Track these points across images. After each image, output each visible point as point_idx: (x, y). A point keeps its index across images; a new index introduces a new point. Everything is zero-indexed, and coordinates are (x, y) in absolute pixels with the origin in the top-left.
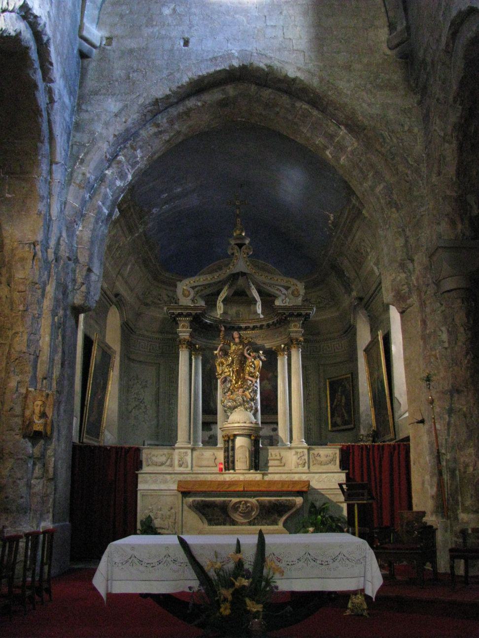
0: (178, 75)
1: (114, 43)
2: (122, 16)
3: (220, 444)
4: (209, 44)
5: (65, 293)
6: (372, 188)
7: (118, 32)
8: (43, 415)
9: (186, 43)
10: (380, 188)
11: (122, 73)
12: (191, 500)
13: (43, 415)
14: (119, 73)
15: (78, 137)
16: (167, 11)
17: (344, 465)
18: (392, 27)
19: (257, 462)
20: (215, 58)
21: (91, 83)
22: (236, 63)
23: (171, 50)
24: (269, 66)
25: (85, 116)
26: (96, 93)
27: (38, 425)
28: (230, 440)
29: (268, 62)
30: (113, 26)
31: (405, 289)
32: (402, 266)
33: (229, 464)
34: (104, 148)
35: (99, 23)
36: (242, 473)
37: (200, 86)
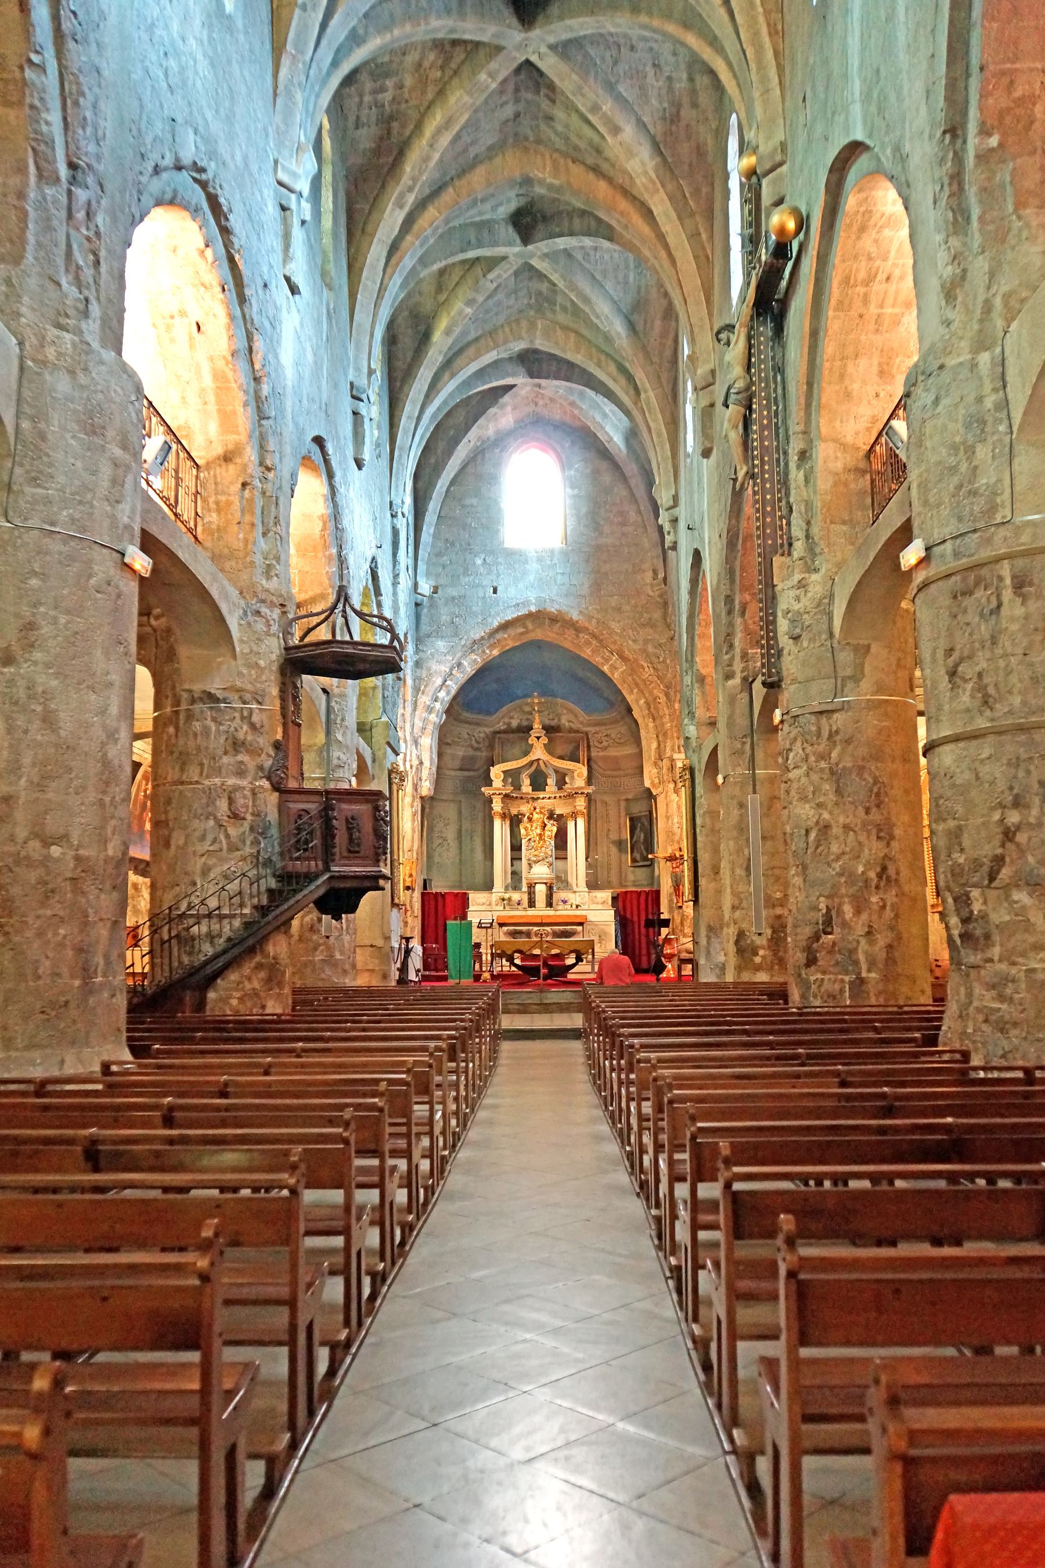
0: (490, 620)
1: (440, 591)
2: (444, 567)
3: (525, 889)
4: (512, 592)
5: (416, 790)
6: (637, 701)
7: (442, 581)
8: (411, 875)
9: (495, 591)
10: (642, 702)
11: (448, 619)
12: (505, 929)
13: (411, 875)
14: (445, 618)
16: (479, 561)
18: (655, 572)
20: (518, 605)
21: (425, 628)
22: (533, 609)
24: (559, 611)
25: (421, 654)
26: (429, 636)
28: (531, 887)
29: (557, 607)
30: (438, 575)
31: (656, 781)
32: (655, 764)
33: (532, 904)
34: (439, 681)
35: (428, 575)
36: (541, 910)
37: (505, 626)
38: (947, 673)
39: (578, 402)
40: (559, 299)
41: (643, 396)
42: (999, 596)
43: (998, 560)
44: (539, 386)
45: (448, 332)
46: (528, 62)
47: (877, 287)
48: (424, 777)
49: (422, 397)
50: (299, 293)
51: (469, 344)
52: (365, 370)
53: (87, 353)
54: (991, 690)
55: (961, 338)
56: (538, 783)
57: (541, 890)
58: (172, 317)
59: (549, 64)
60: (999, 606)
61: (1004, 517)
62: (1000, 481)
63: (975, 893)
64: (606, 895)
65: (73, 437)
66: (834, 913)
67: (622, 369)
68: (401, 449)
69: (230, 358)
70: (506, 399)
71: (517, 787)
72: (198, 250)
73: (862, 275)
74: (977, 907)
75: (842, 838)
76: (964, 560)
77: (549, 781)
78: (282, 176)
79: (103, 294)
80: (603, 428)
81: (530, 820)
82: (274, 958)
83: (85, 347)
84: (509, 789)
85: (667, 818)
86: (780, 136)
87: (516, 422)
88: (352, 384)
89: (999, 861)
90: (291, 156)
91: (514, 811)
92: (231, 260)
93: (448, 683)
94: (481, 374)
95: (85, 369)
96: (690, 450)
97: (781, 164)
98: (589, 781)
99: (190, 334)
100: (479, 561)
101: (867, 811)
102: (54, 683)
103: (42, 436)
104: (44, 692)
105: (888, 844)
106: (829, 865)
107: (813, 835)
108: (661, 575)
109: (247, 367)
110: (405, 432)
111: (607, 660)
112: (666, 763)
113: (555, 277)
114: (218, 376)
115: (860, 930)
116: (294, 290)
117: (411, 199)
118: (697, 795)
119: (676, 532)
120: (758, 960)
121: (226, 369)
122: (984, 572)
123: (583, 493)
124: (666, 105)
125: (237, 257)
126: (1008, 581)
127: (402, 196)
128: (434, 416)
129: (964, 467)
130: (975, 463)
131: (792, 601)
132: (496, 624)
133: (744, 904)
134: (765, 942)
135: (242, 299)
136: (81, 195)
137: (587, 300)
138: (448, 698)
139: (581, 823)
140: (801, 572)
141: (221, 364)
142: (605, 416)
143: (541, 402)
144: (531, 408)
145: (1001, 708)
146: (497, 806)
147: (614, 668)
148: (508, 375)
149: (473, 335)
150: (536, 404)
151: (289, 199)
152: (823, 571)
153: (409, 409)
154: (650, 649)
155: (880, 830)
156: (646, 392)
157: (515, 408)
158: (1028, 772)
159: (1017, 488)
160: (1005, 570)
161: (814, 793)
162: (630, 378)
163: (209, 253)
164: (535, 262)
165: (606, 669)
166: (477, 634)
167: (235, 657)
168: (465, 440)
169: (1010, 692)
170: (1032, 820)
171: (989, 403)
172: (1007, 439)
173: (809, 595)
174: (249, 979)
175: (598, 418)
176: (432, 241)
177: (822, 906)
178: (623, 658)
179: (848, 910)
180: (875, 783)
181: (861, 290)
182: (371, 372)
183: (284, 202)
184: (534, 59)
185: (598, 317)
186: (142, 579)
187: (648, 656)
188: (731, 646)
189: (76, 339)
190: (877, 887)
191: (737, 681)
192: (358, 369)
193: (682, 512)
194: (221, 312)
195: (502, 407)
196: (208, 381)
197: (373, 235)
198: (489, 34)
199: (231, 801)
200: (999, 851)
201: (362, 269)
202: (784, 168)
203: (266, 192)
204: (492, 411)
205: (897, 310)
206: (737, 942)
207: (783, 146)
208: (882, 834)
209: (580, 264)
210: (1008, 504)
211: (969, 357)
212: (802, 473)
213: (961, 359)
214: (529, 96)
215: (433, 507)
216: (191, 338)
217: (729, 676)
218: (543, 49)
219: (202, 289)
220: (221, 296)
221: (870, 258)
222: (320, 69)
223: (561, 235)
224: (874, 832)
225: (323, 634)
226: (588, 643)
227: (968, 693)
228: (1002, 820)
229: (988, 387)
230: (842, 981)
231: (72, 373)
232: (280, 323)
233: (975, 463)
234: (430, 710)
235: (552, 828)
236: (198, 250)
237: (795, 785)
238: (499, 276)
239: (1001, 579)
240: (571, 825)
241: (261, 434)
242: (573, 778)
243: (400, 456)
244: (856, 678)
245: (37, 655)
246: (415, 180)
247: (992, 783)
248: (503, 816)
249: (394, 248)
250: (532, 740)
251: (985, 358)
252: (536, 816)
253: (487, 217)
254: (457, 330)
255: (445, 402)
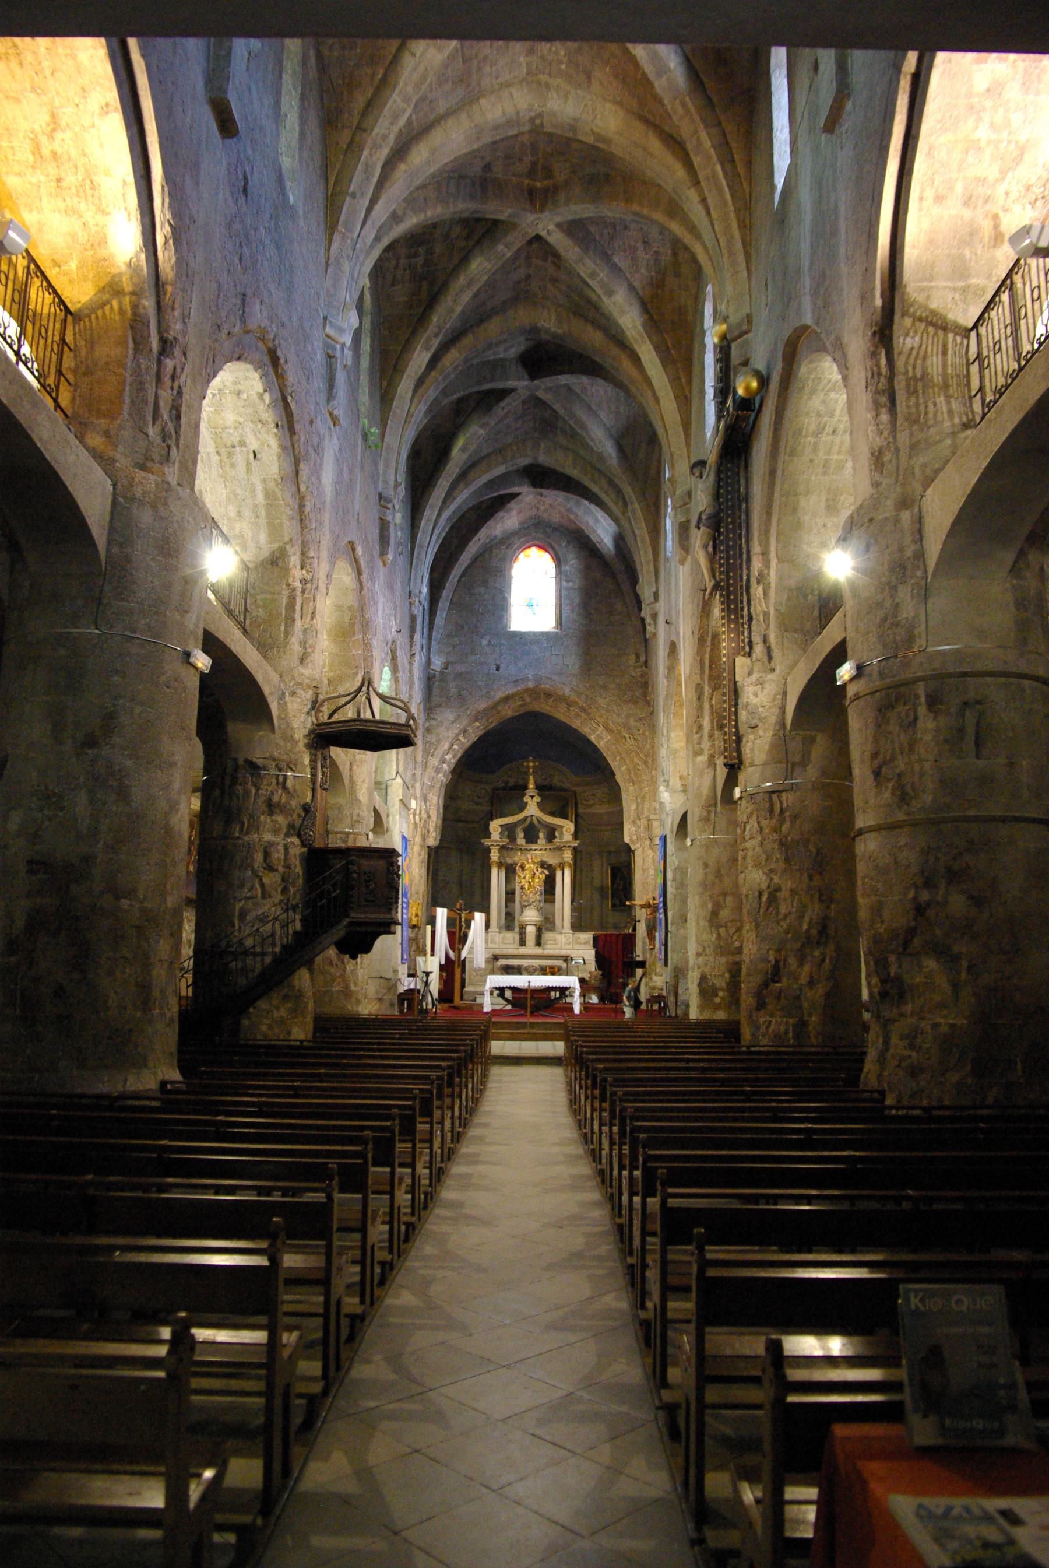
2: (454, 646)
3: (517, 930)
6: (620, 767)
7: (452, 659)
9: (498, 669)
10: (623, 768)
13: (417, 915)
15: (429, 738)
16: (484, 642)
17: (595, 946)
18: (638, 656)
19: (539, 943)
20: (517, 681)
21: (436, 700)
22: (531, 685)
23: (488, 674)
25: (434, 723)
26: (440, 706)
27: (414, 922)
28: (522, 928)
30: (448, 653)
31: (635, 837)
32: (634, 822)
33: (522, 942)
34: (446, 747)
37: (507, 699)
38: (873, 772)
39: (575, 509)
40: (560, 424)
41: (630, 508)
42: (915, 712)
43: (915, 681)
44: (541, 495)
45: (463, 449)
46: (538, 238)
47: (824, 438)
48: (432, 830)
49: (440, 503)
50: (340, 424)
51: (483, 458)
52: (392, 483)
53: (167, 491)
54: (908, 789)
55: (886, 498)
56: (531, 837)
57: (531, 930)
58: (234, 447)
59: (557, 239)
60: (916, 719)
61: (920, 646)
62: (916, 616)
63: (892, 958)
64: (588, 937)
65: (153, 559)
66: (781, 964)
67: (611, 483)
68: (421, 546)
69: (279, 480)
70: (513, 505)
71: (512, 838)
72: (258, 393)
73: (812, 427)
74: (893, 970)
75: (789, 901)
76: (888, 680)
77: (541, 835)
78: (328, 330)
79: (182, 442)
80: (595, 531)
81: (523, 868)
82: (299, 990)
83: (165, 486)
84: (505, 841)
85: (644, 870)
86: (746, 310)
87: (520, 523)
88: (380, 495)
89: (911, 932)
90: (338, 314)
91: (509, 861)
92: (284, 400)
93: (455, 747)
94: (491, 484)
95: (166, 504)
96: (668, 554)
97: (746, 333)
98: (576, 836)
99: (248, 460)
100: (484, 642)
101: (811, 878)
102: (129, 763)
103: (128, 559)
104: (120, 770)
105: (828, 907)
106: (778, 923)
107: (765, 898)
108: (643, 659)
109: (295, 489)
110: (424, 532)
111: (594, 732)
112: (644, 822)
113: (556, 407)
114: (268, 494)
115: (803, 979)
116: (335, 420)
117: (435, 343)
118: (669, 852)
119: (655, 623)
120: (717, 1000)
121: (277, 490)
122: (902, 689)
123: (576, 586)
124: (653, 274)
125: (289, 399)
126: (923, 699)
127: (428, 340)
128: (449, 519)
129: (888, 603)
130: (897, 600)
131: (752, 697)
132: (499, 695)
133: (708, 951)
134: (724, 985)
135: (292, 431)
136: (169, 363)
137: (584, 427)
138: (454, 761)
139: (568, 873)
140: (759, 672)
141: (272, 485)
142: (597, 521)
143: (542, 508)
144: (535, 511)
145: (916, 804)
146: (494, 856)
147: (599, 737)
148: (514, 485)
149: (485, 452)
150: (538, 509)
151: (334, 349)
152: (777, 671)
153: (429, 514)
154: (632, 722)
155: (821, 895)
156: (632, 503)
157: (519, 513)
158: (937, 859)
159: (930, 624)
160: (921, 689)
161: (766, 860)
162: (619, 492)
163: (267, 397)
164: (541, 394)
165: (593, 738)
166: (482, 705)
167: (273, 730)
168: (476, 538)
169: (923, 791)
170: (939, 898)
171: (909, 553)
172: (923, 583)
173: (765, 691)
174: (278, 1009)
175: (591, 523)
176: (452, 376)
177: (772, 958)
178: (607, 728)
179: (793, 962)
180: (818, 853)
181: (811, 439)
182: (397, 485)
183: (330, 352)
184: (543, 234)
185: (592, 440)
186: (202, 674)
187: (629, 728)
188: (700, 727)
189: (160, 480)
190: (818, 943)
191: (703, 759)
192: (386, 482)
193: (661, 607)
194: (274, 443)
195: (509, 511)
196: (260, 498)
197: (403, 372)
198: (506, 214)
199: (267, 855)
200: (912, 924)
201: (392, 400)
202: (750, 336)
203: (316, 343)
204: (501, 514)
205: (842, 457)
206: (699, 985)
207: (749, 319)
208: (824, 898)
209: (579, 397)
210: (924, 635)
211: (893, 513)
212: (760, 589)
213: (887, 515)
214: (540, 263)
215: (446, 594)
216: (248, 464)
217: (697, 754)
218: (551, 227)
219: (260, 425)
220: (275, 430)
221: (819, 415)
222: (365, 243)
223: (562, 373)
224: (817, 895)
225: (350, 713)
226: (578, 715)
227: (889, 791)
228: (915, 898)
229: (908, 540)
230: (787, 1023)
231: (154, 507)
232: (323, 450)
233: (897, 600)
234: (438, 770)
235: (541, 875)
236: (258, 393)
237: (750, 853)
238: (508, 404)
239: (917, 697)
240: (559, 874)
241: (303, 542)
242: (562, 833)
243: (419, 554)
244: (805, 761)
245: (117, 740)
246: (440, 328)
247: (908, 866)
248: (500, 865)
249: (420, 382)
250: (527, 799)
251: (906, 516)
252: (527, 866)
253: (501, 356)
254: (472, 448)
255: (459, 508)
